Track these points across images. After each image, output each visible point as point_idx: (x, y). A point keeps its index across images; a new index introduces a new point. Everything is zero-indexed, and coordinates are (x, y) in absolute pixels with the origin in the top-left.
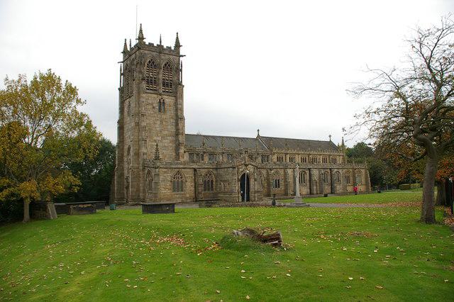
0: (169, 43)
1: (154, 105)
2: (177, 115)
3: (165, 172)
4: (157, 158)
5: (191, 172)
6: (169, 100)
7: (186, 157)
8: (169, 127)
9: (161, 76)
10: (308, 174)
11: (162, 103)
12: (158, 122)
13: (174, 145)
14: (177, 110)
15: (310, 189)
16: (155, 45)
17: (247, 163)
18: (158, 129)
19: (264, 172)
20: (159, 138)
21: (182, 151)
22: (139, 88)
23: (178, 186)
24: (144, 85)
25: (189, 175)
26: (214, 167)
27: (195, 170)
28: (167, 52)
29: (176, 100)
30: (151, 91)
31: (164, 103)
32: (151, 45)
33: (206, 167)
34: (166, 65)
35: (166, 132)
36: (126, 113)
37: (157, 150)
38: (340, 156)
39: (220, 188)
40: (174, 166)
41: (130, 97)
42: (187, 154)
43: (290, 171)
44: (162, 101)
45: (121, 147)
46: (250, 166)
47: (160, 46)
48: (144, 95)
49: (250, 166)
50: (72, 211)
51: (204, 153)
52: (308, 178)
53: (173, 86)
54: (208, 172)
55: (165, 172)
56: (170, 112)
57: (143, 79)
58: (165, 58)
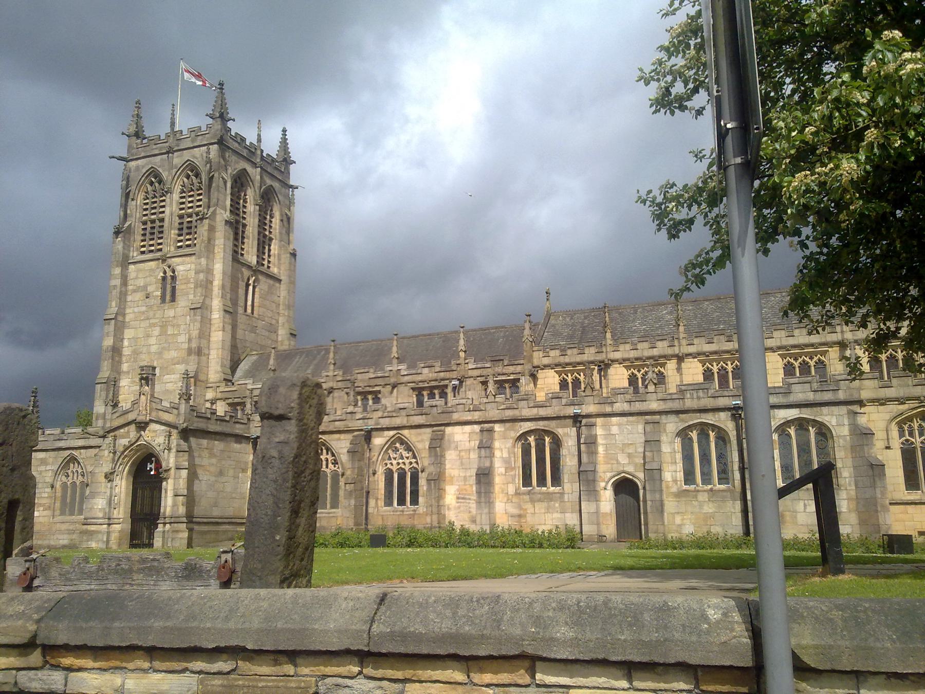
1: (150, 289)
12: (156, 331)
30: (150, 256)
31: (174, 278)
35: (173, 354)
40: (62, 444)
44: (169, 273)
46: (153, 426)
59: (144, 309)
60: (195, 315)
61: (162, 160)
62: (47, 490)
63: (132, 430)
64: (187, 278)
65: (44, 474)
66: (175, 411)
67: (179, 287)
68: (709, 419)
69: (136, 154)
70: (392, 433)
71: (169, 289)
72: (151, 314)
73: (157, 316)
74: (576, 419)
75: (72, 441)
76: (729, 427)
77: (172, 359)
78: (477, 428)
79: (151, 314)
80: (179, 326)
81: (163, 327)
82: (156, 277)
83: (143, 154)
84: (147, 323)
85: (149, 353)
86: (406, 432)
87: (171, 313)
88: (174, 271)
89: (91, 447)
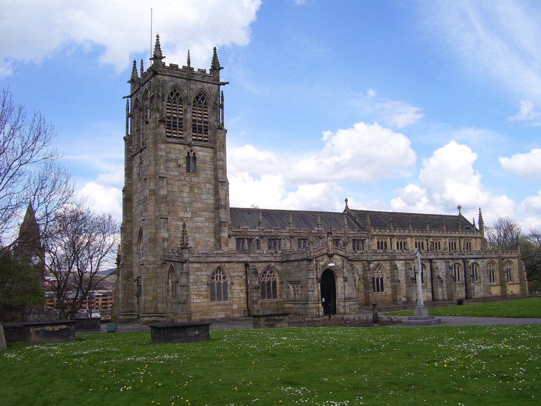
0: (202, 62)
2: (216, 178)
3: (198, 269)
4: (184, 246)
5: (241, 267)
6: (203, 154)
7: (232, 245)
8: (204, 197)
9: (189, 116)
10: (428, 268)
11: (191, 159)
12: (187, 189)
13: (212, 226)
14: (216, 169)
15: (433, 292)
16: (180, 67)
17: (331, 252)
18: (186, 200)
19: (359, 266)
20: (189, 215)
21: (225, 235)
22: (155, 135)
23: (218, 291)
24: (163, 130)
25: (236, 273)
26: (278, 259)
27: (247, 264)
28: (199, 78)
29: (215, 153)
31: (195, 158)
32: (173, 67)
33: (265, 259)
34: (197, 98)
35: (199, 205)
36: (135, 177)
37: (184, 233)
38: (476, 238)
39: (288, 294)
40: (212, 259)
41: (141, 151)
42: (233, 239)
43: (400, 264)
44: (191, 155)
45: (128, 230)
46: (336, 257)
47: (188, 69)
48: (163, 146)
49: (336, 257)
50: (33, 337)
51: (262, 237)
52: (429, 275)
53: (211, 134)
54: (268, 268)
55: (198, 269)
56: (206, 173)
57: (162, 121)
58: (197, 87)
59: (177, 173)
60: (222, 185)
62: (203, 286)
63: (326, 259)
65: (200, 277)
66: (344, 250)
68: (458, 261)
69: (163, 72)
70: (376, 262)
72: (182, 178)
73: (187, 180)
74: (430, 260)
75: (219, 258)
76: (462, 264)
78: (403, 262)
79: (182, 178)
80: (202, 189)
81: (191, 189)
83: (168, 74)
84: (180, 183)
85: (183, 202)
86: (381, 262)
87: (196, 180)
88: (194, 154)
89: (232, 262)
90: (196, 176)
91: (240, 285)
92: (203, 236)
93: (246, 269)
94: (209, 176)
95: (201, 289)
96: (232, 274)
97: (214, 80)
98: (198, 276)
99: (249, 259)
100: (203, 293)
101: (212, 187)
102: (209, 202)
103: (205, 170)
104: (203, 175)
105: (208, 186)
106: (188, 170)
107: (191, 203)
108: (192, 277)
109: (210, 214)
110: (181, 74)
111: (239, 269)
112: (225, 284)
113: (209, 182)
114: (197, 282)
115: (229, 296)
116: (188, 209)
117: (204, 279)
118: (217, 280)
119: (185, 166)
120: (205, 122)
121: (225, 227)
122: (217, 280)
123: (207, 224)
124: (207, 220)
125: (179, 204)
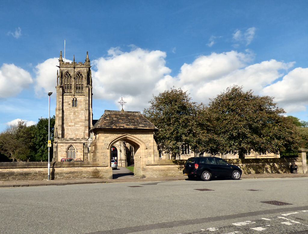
1: (69, 103)
3: (62, 146)
8: (80, 116)
12: (73, 114)
18: (72, 118)
20: (73, 124)
28: (79, 66)
31: (76, 100)
35: (78, 120)
44: (75, 99)
55: (62, 146)
59: (68, 107)
61: (71, 69)
64: (81, 101)
65: (63, 149)
67: (78, 103)
69: (62, 66)
71: (74, 103)
77: (78, 121)
79: (71, 109)
80: (79, 113)
81: (75, 113)
82: (71, 100)
84: (69, 111)
85: (71, 119)
87: (77, 109)
88: (76, 99)
89: (77, 143)
90: (77, 108)
91: (81, 152)
92: (79, 132)
93: (84, 146)
94: (83, 108)
95: (63, 154)
96: (77, 148)
97: (86, 66)
98: (62, 148)
99: (85, 142)
100: (63, 155)
101: (84, 112)
102: (82, 118)
103: (81, 105)
104: (80, 107)
105: (82, 112)
106: (73, 106)
107: (74, 119)
108: (59, 149)
109: (83, 123)
110: (71, 66)
111: (80, 146)
112: (74, 152)
113: (82, 110)
114: (61, 151)
115: (76, 157)
116: (73, 122)
117: (65, 150)
118: (71, 150)
119: (72, 104)
120: (82, 85)
121: (87, 128)
122: (71, 150)
123: (81, 127)
124: (81, 126)
125: (69, 120)
